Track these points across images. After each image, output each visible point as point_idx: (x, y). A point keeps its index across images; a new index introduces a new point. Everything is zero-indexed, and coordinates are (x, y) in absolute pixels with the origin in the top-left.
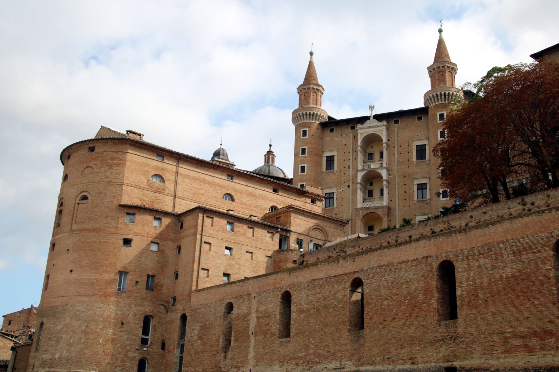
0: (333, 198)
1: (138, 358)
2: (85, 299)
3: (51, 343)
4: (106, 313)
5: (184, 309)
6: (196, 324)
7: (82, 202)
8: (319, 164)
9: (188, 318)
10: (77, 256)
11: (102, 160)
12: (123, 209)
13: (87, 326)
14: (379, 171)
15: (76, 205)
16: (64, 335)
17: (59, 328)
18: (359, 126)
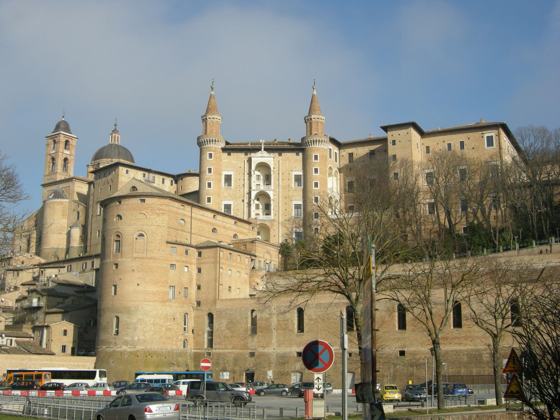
0: (230, 208)
1: (183, 340)
2: (152, 303)
3: (129, 330)
4: (164, 313)
5: (209, 310)
6: (223, 320)
7: (139, 238)
8: (220, 180)
9: (215, 316)
10: (141, 275)
11: (152, 210)
12: (169, 244)
13: (154, 321)
14: (268, 192)
15: (135, 239)
16: (139, 326)
17: (135, 321)
18: (253, 154)
